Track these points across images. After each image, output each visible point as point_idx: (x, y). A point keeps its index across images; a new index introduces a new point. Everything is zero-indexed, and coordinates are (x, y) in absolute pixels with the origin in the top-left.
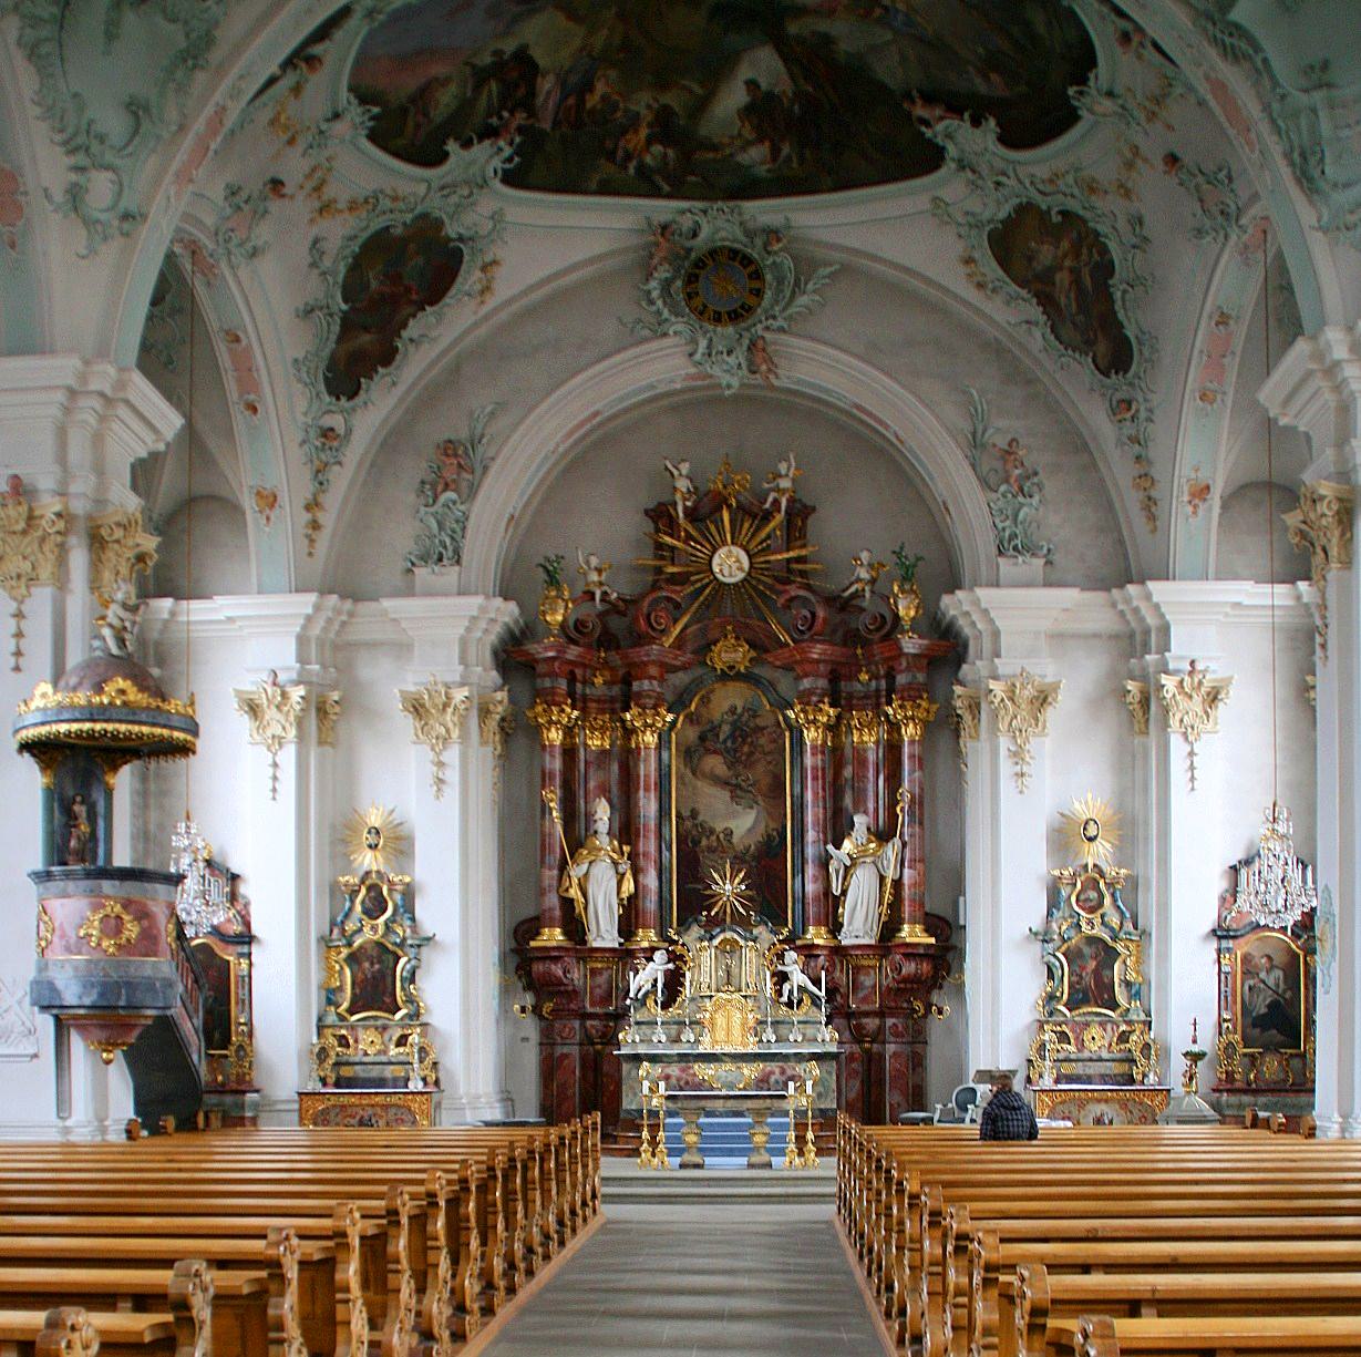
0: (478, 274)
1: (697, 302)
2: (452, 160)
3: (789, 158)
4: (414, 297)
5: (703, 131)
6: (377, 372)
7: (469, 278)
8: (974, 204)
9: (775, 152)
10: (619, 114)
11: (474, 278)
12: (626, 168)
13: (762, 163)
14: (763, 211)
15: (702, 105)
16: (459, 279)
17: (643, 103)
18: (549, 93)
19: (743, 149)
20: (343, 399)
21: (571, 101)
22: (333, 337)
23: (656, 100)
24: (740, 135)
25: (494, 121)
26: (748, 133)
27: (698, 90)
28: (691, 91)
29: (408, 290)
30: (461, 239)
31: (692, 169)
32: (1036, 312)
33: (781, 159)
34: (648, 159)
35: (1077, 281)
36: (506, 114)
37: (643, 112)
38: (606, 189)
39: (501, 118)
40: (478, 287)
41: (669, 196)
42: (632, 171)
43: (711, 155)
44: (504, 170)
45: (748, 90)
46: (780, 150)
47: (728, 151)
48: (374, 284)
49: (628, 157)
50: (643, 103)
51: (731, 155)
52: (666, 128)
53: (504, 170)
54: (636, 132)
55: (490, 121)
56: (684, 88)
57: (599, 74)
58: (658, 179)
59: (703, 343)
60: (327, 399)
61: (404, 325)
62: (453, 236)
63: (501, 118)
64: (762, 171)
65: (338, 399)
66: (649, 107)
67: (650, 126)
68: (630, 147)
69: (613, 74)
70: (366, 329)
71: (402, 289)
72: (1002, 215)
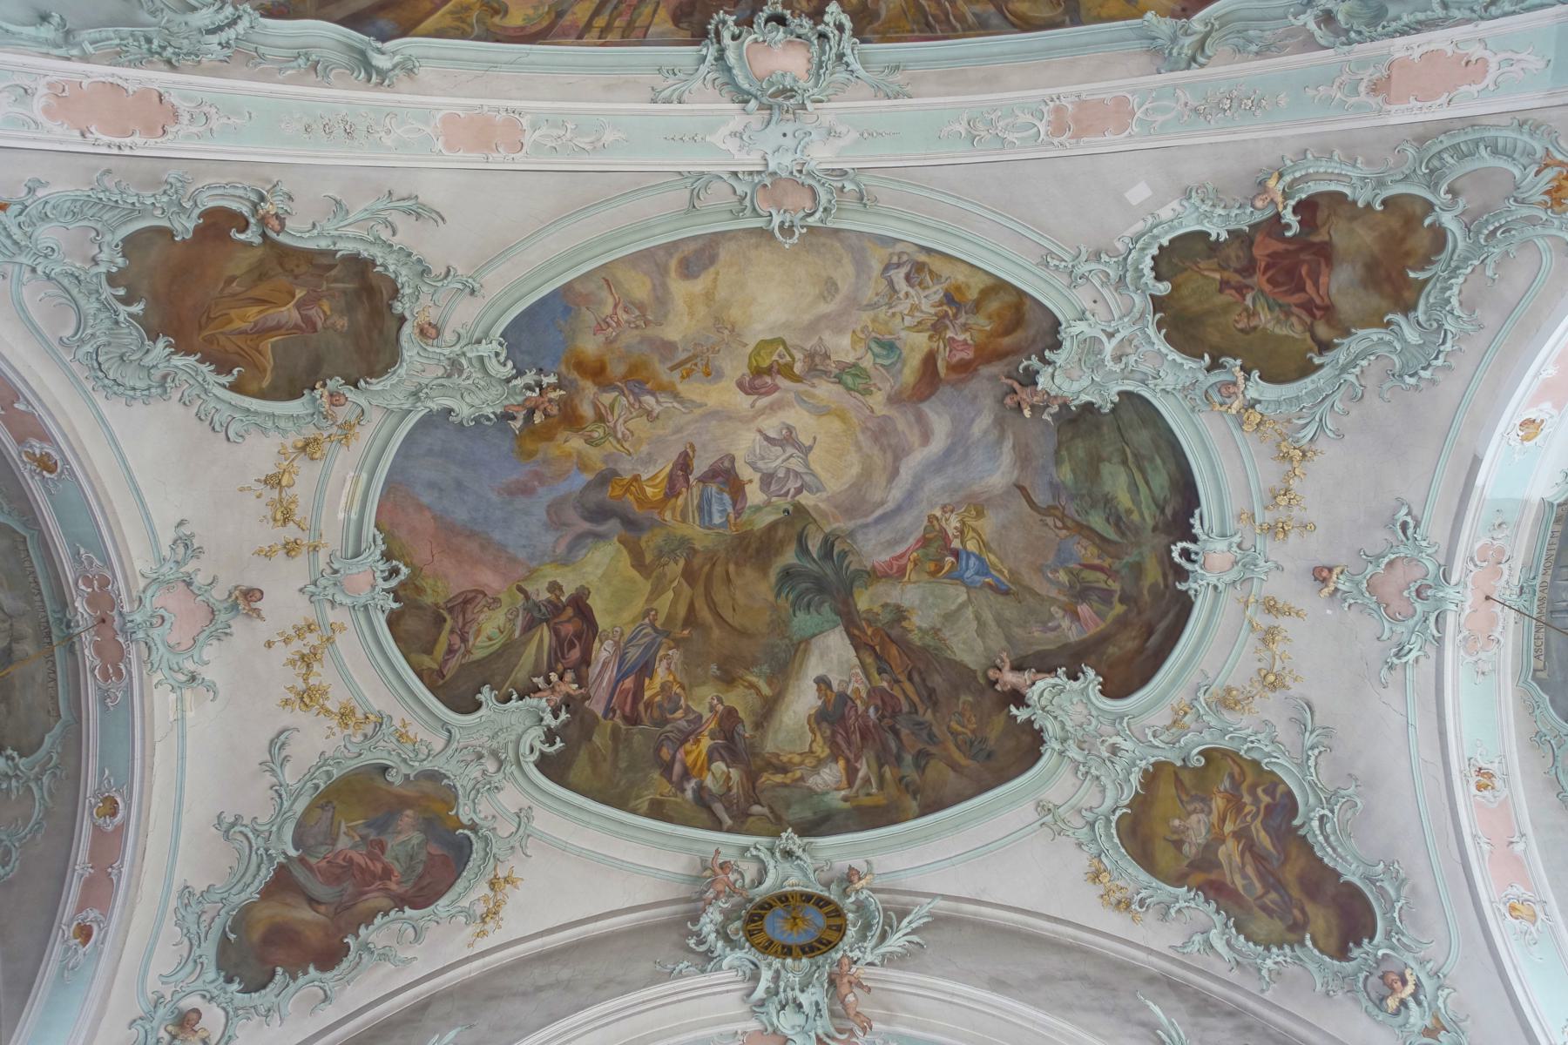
0: (483, 889)
1: (759, 939)
2: (483, 711)
3: (867, 781)
4: (393, 886)
5: (770, 747)
6: (305, 973)
7: (470, 892)
8: (1088, 796)
9: (851, 772)
10: (679, 714)
11: (473, 896)
12: (683, 790)
13: (837, 789)
14: (837, 851)
15: (768, 710)
16: (460, 885)
17: (705, 700)
18: (605, 664)
19: (816, 769)
20: (235, 986)
21: (629, 683)
22: (258, 885)
23: (720, 701)
24: (811, 752)
25: (539, 681)
26: (822, 750)
27: (766, 690)
28: (758, 692)
29: (387, 873)
30: (474, 827)
31: (753, 795)
32: (1202, 910)
33: (858, 782)
34: (708, 781)
35: (1250, 847)
36: (554, 677)
37: (707, 715)
38: (657, 811)
39: (548, 681)
40: (480, 909)
41: (729, 831)
42: (689, 794)
43: (779, 778)
44: (542, 753)
45: (819, 690)
46: (857, 770)
47: (798, 774)
48: (343, 843)
49: (686, 774)
50: (705, 700)
51: (802, 779)
52: (730, 744)
53: (542, 753)
54: (697, 741)
55: (535, 680)
56: (752, 686)
57: (661, 653)
58: (718, 808)
59: (766, 976)
60: (211, 974)
61: (368, 919)
62: (465, 820)
63: (548, 681)
64: (836, 799)
65: (229, 980)
66: (712, 709)
67: (712, 736)
68: (690, 760)
69: (675, 654)
70: (313, 902)
71: (379, 866)
72: (1126, 798)
